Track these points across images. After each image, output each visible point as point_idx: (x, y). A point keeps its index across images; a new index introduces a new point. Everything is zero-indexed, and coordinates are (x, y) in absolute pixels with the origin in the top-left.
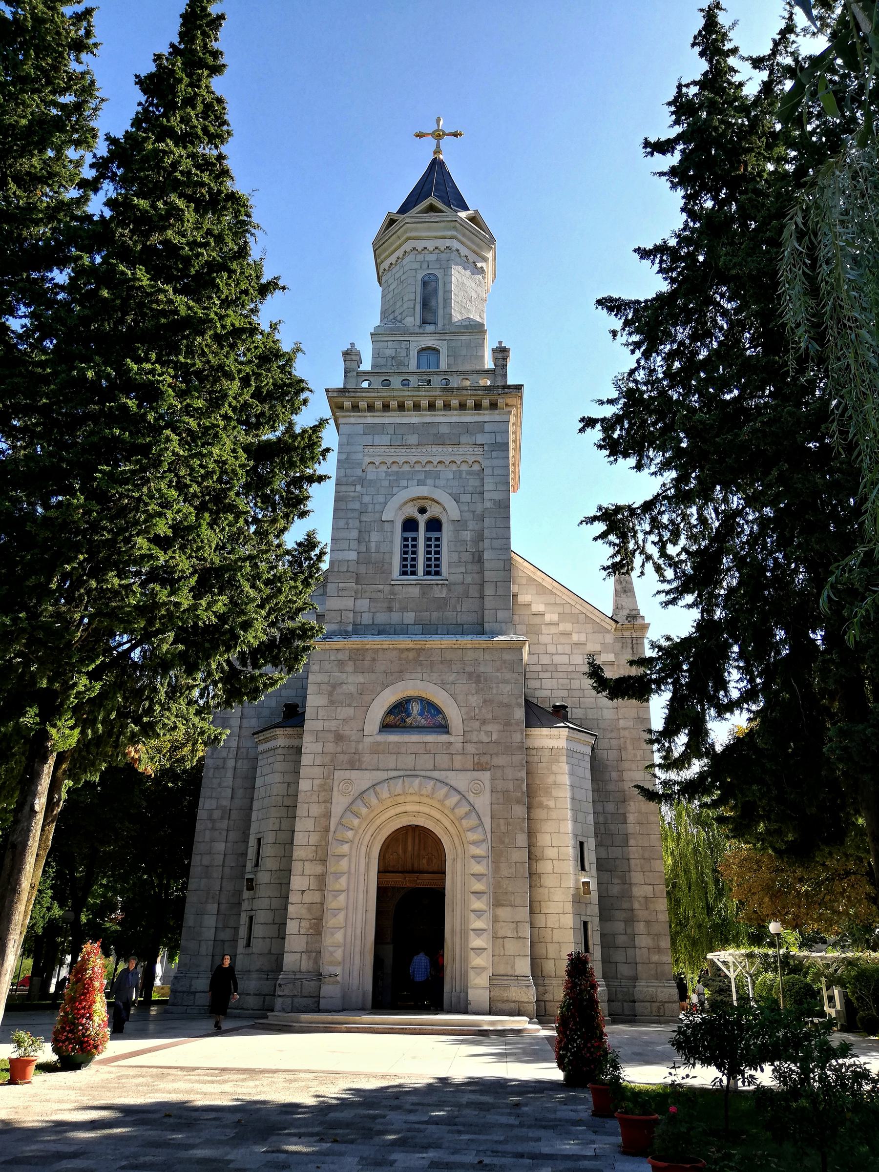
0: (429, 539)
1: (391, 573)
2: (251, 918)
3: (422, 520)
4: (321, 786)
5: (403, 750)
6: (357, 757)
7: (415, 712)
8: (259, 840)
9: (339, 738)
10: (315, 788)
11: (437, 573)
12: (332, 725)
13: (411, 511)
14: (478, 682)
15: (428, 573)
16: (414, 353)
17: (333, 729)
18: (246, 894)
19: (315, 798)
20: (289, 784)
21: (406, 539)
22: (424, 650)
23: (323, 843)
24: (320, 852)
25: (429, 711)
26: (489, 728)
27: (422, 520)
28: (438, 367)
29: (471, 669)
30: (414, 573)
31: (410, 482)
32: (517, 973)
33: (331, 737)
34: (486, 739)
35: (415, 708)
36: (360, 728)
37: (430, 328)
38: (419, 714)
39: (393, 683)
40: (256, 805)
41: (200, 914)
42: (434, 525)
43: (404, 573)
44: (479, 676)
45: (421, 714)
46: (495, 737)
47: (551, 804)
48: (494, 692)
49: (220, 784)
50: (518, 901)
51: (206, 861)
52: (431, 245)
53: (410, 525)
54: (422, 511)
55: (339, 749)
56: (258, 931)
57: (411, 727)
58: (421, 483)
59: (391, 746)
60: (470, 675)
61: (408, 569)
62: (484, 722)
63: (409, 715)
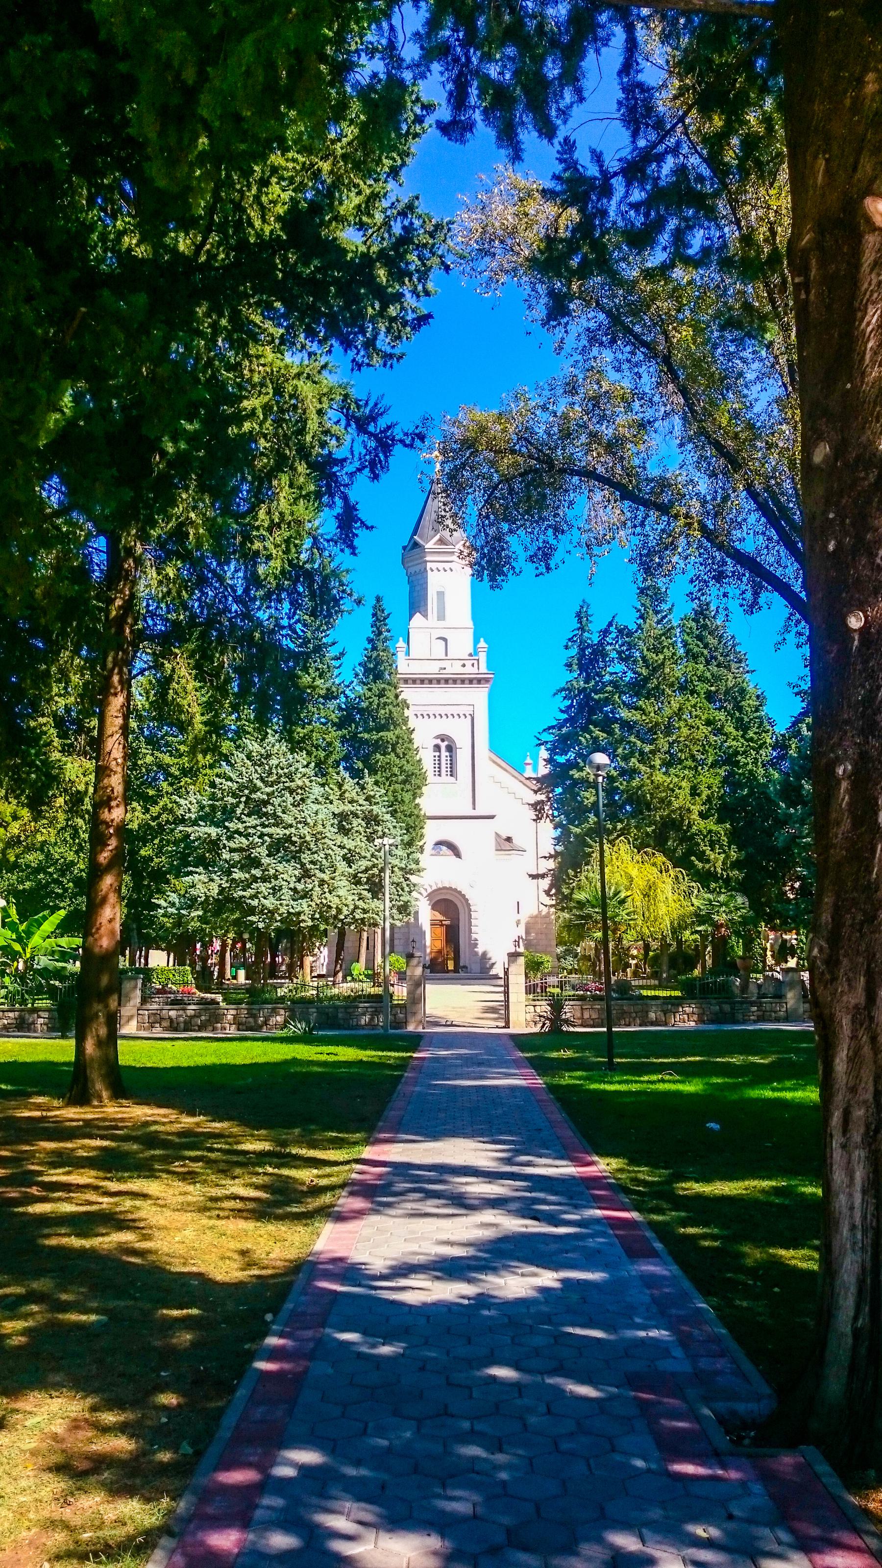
37: (441, 624)
42: (450, 749)
52: (441, 566)
54: (443, 740)
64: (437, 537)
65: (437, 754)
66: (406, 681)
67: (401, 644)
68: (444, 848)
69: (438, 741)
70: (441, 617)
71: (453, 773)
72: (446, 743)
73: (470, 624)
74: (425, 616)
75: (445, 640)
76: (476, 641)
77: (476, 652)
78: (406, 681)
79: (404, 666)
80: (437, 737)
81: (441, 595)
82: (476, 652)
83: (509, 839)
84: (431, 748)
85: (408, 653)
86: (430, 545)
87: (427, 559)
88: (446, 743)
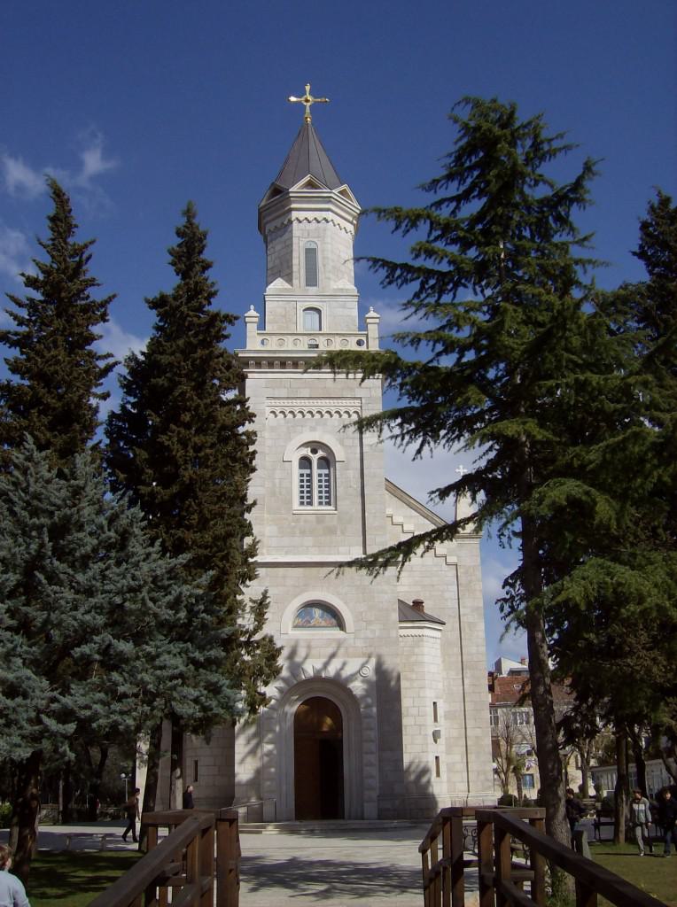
0: (320, 475)
1: (290, 502)
2: (196, 762)
3: (315, 458)
7: (317, 615)
11: (329, 503)
13: (307, 452)
15: (321, 503)
16: (300, 312)
21: (302, 475)
27: (315, 458)
28: (320, 329)
30: (310, 503)
31: (304, 428)
34: (370, 636)
37: (313, 290)
42: (327, 462)
43: (302, 503)
46: (377, 634)
47: (414, 676)
53: (305, 462)
54: (314, 451)
56: (201, 771)
57: (314, 626)
58: (313, 429)
61: (307, 499)
62: (369, 623)
63: (313, 618)
64: (307, 178)
65: (308, 471)
66: (258, 363)
67: (252, 312)
68: (317, 612)
69: (307, 452)
70: (312, 280)
71: (329, 498)
72: (321, 453)
73: (355, 291)
74: (289, 279)
75: (318, 311)
76: (363, 311)
77: (363, 326)
78: (258, 363)
79: (254, 344)
80: (306, 445)
81: (311, 254)
82: (363, 326)
83: (418, 604)
84: (296, 464)
85: (262, 325)
86: (295, 189)
87: (293, 206)
88: (321, 453)
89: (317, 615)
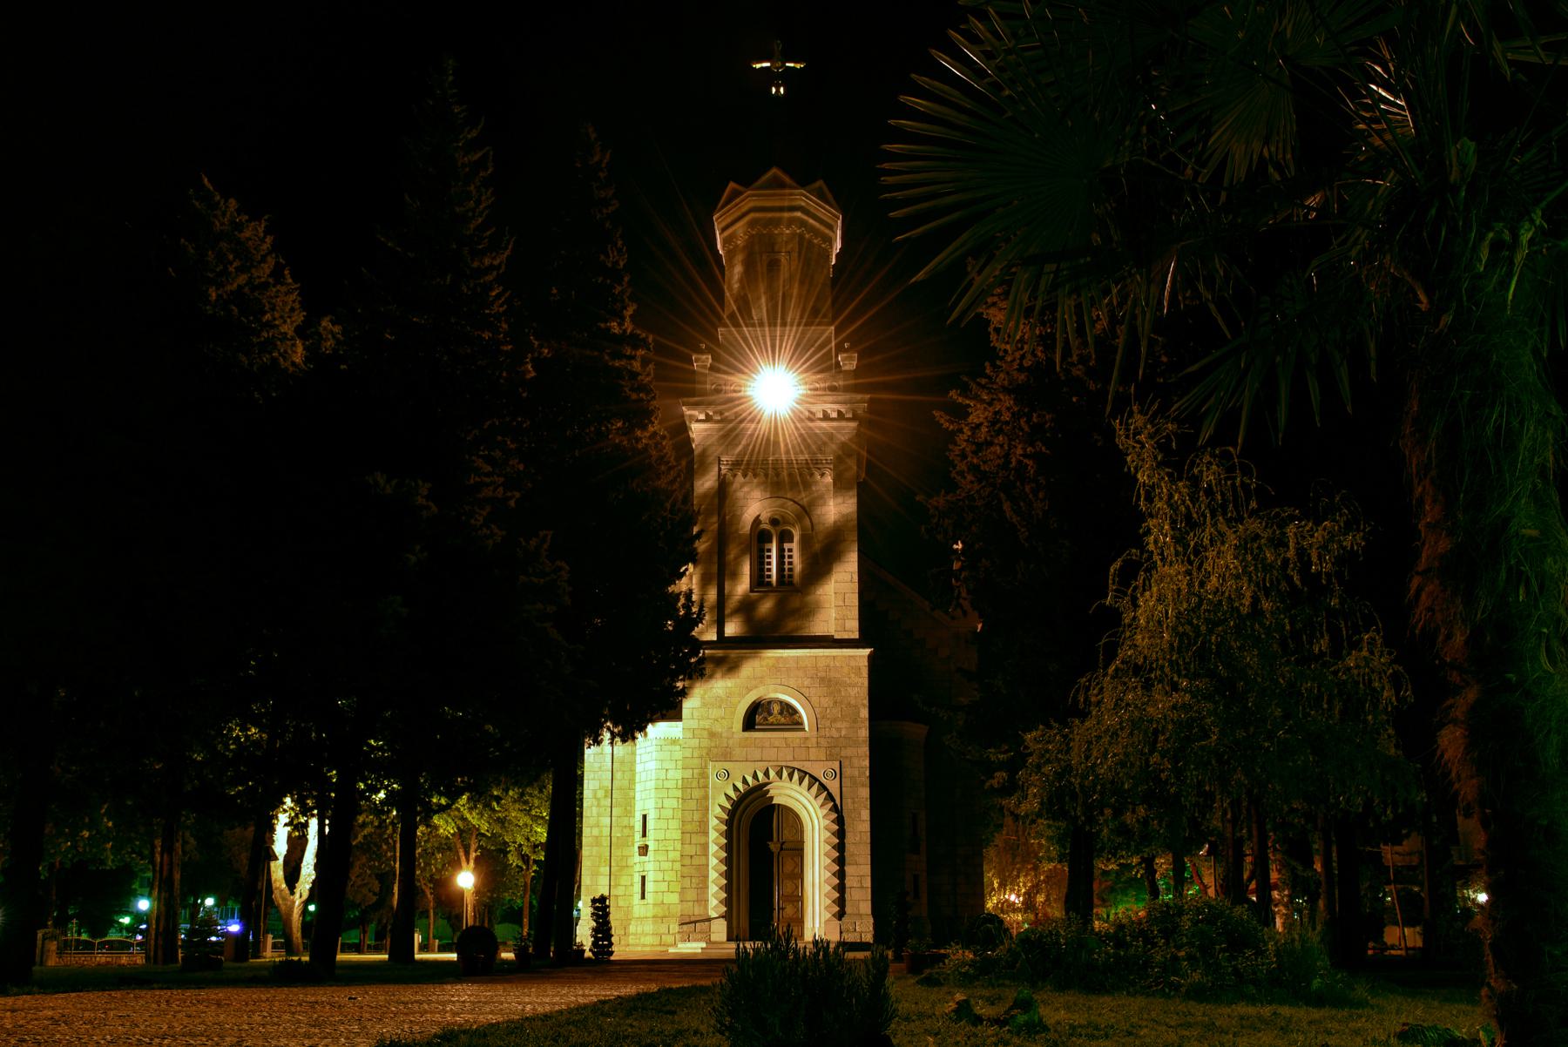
4: (700, 774)
5: (767, 744)
6: (728, 749)
7: (776, 712)
8: (645, 817)
9: (712, 735)
10: (695, 776)
12: (707, 724)
14: (829, 686)
17: (707, 727)
18: (637, 858)
19: (695, 784)
20: (667, 770)
22: (782, 657)
23: (705, 820)
24: (702, 827)
25: (788, 711)
26: (839, 725)
29: (823, 674)
32: (861, 912)
33: (705, 734)
34: (835, 734)
35: (776, 708)
36: (730, 726)
38: (779, 714)
39: (756, 687)
40: (638, 787)
41: (595, 874)
44: (830, 680)
45: (781, 713)
48: (843, 694)
49: (600, 768)
50: (861, 860)
51: (596, 832)
55: (713, 745)
56: (649, 887)
59: (757, 741)
60: (822, 679)
62: (834, 720)
63: (770, 714)
89: (776, 712)
